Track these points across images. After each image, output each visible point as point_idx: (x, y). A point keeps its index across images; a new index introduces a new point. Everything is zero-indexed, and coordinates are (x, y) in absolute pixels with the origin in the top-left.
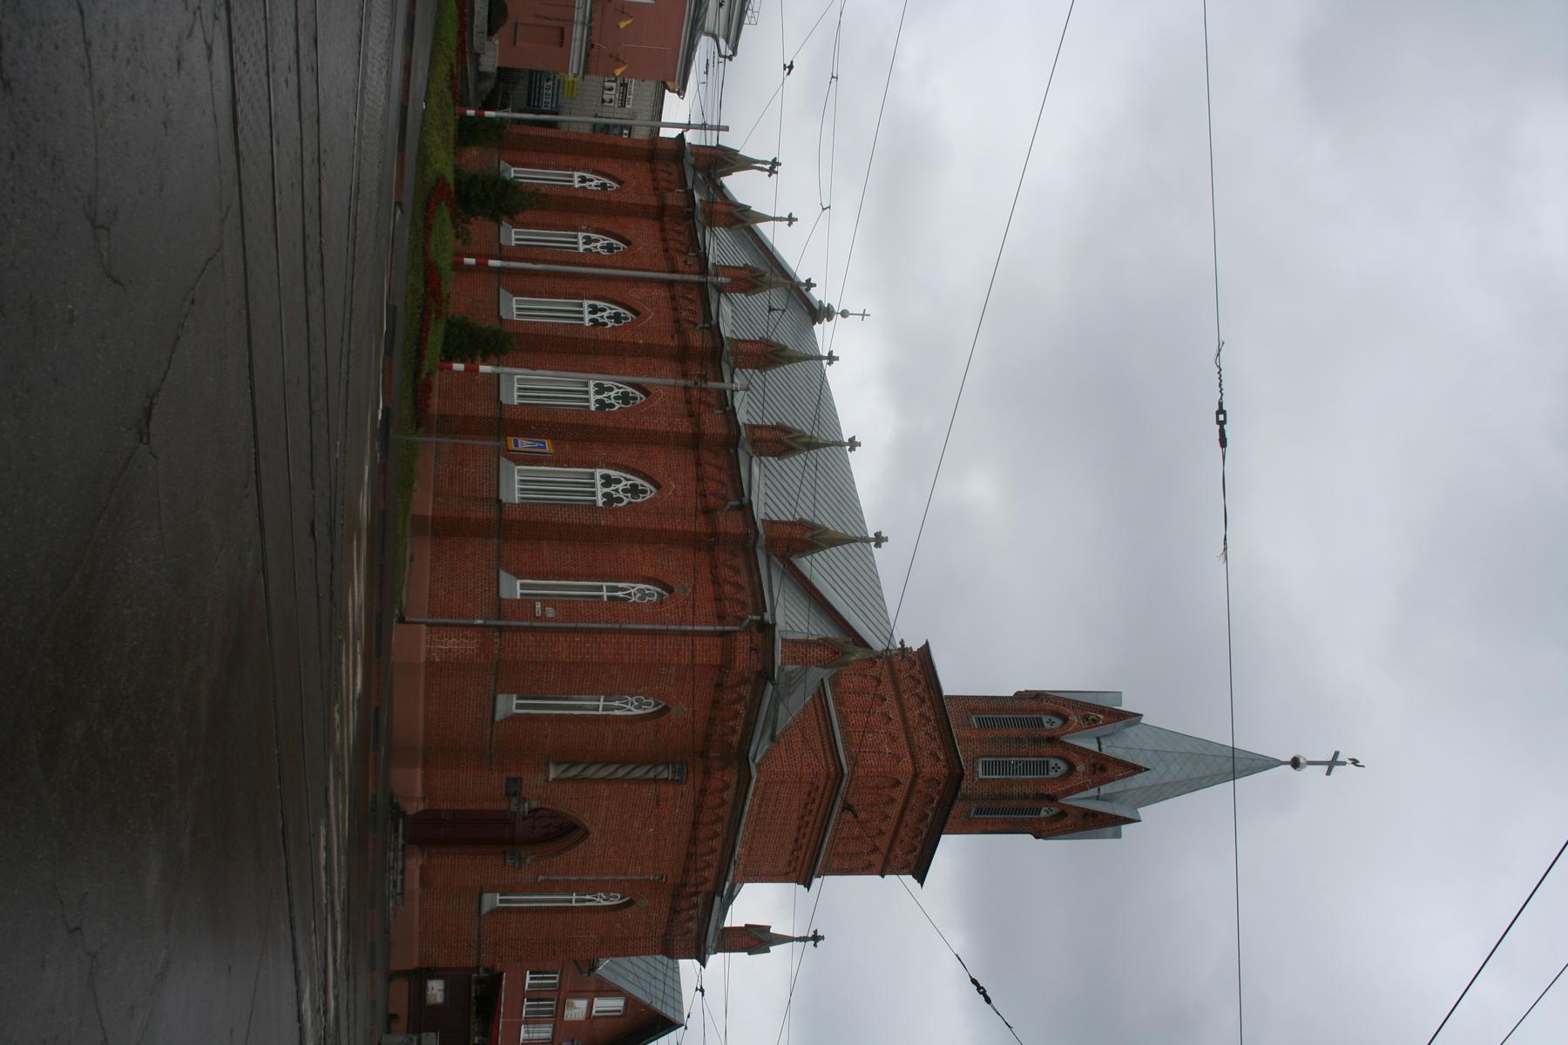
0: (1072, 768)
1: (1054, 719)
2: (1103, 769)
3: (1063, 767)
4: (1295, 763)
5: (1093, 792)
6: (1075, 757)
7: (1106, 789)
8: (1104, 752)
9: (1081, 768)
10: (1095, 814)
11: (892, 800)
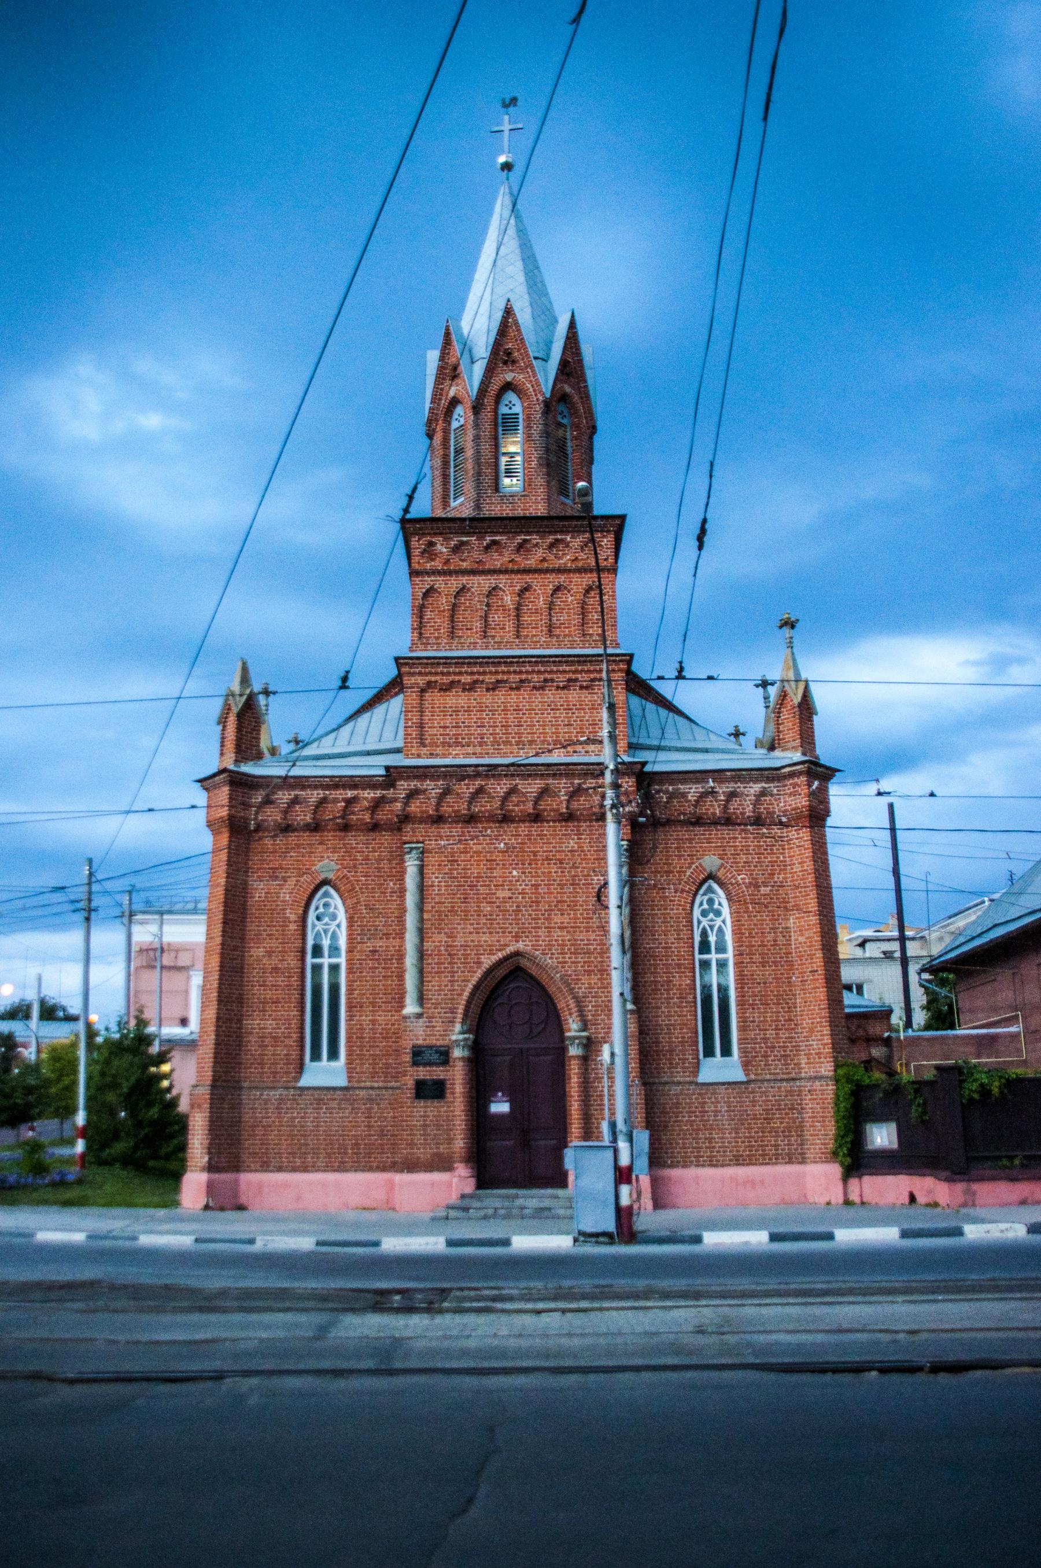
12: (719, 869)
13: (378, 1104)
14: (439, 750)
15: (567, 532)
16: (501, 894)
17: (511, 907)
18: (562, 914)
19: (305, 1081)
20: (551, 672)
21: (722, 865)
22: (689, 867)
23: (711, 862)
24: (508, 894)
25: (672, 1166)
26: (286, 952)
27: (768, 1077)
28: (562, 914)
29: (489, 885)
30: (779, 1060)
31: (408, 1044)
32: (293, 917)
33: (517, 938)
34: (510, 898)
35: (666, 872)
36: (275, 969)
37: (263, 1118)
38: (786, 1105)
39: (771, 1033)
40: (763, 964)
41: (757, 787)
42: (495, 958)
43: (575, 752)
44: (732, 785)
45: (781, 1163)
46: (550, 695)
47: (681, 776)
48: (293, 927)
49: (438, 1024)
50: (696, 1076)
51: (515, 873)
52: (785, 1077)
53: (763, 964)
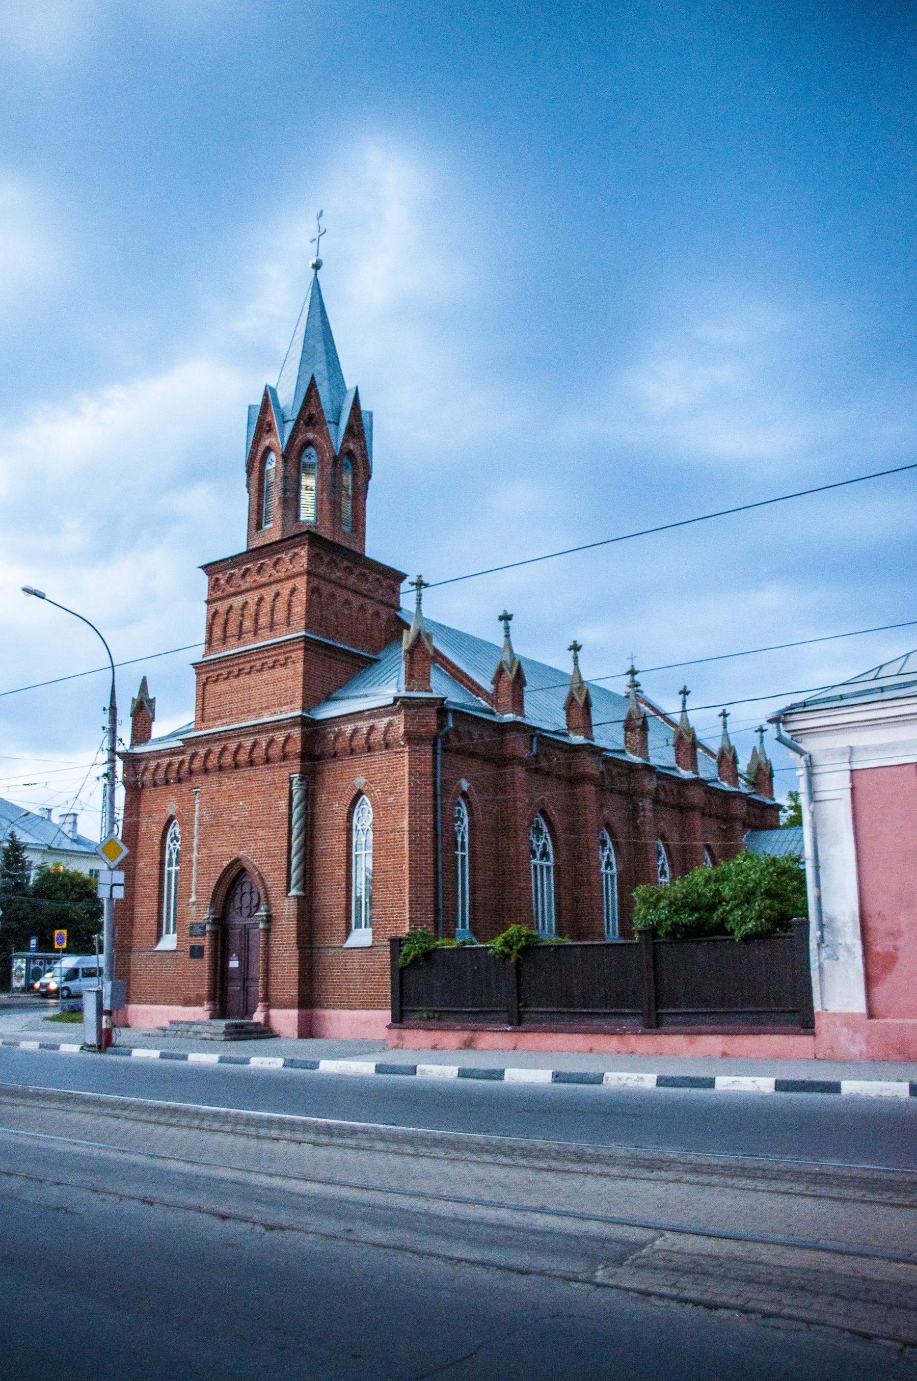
0: (308, 443)
1: (269, 460)
2: (311, 417)
3: (311, 450)
4: (317, 266)
5: (331, 428)
6: (298, 442)
7: (328, 417)
8: (295, 417)
9: (310, 436)
10: (349, 429)
11: (332, 596)
14: (210, 724)
15: (282, 552)
19: (160, 947)
23: (360, 782)
25: (322, 1007)
31: (188, 922)
41: (386, 720)
42: (228, 862)
44: (372, 721)
46: (267, 675)
47: (345, 718)
48: (157, 848)
51: (241, 803)
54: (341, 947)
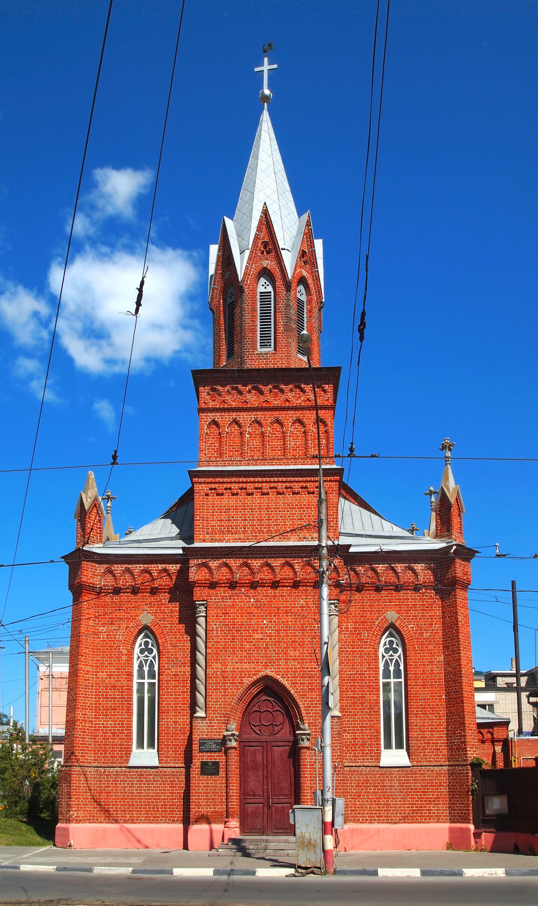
12: (396, 621)
13: (178, 778)
16: (256, 636)
17: (262, 645)
18: (295, 650)
20: (290, 482)
21: (399, 617)
22: (378, 619)
24: (260, 636)
26: (120, 675)
27: (425, 764)
28: (295, 650)
29: (249, 630)
30: (433, 752)
32: (125, 652)
33: (266, 666)
34: (262, 639)
35: (362, 622)
36: (114, 687)
37: (105, 787)
38: (436, 783)
39: (427, 734)
40: (424, 686)
43: (305, 538)
45: (433, 822)
49: (215, 723)
50: (379, 762)
51: (265, 622)
52: (436, 764)
53: (424, 686)
54: (377, 767)
